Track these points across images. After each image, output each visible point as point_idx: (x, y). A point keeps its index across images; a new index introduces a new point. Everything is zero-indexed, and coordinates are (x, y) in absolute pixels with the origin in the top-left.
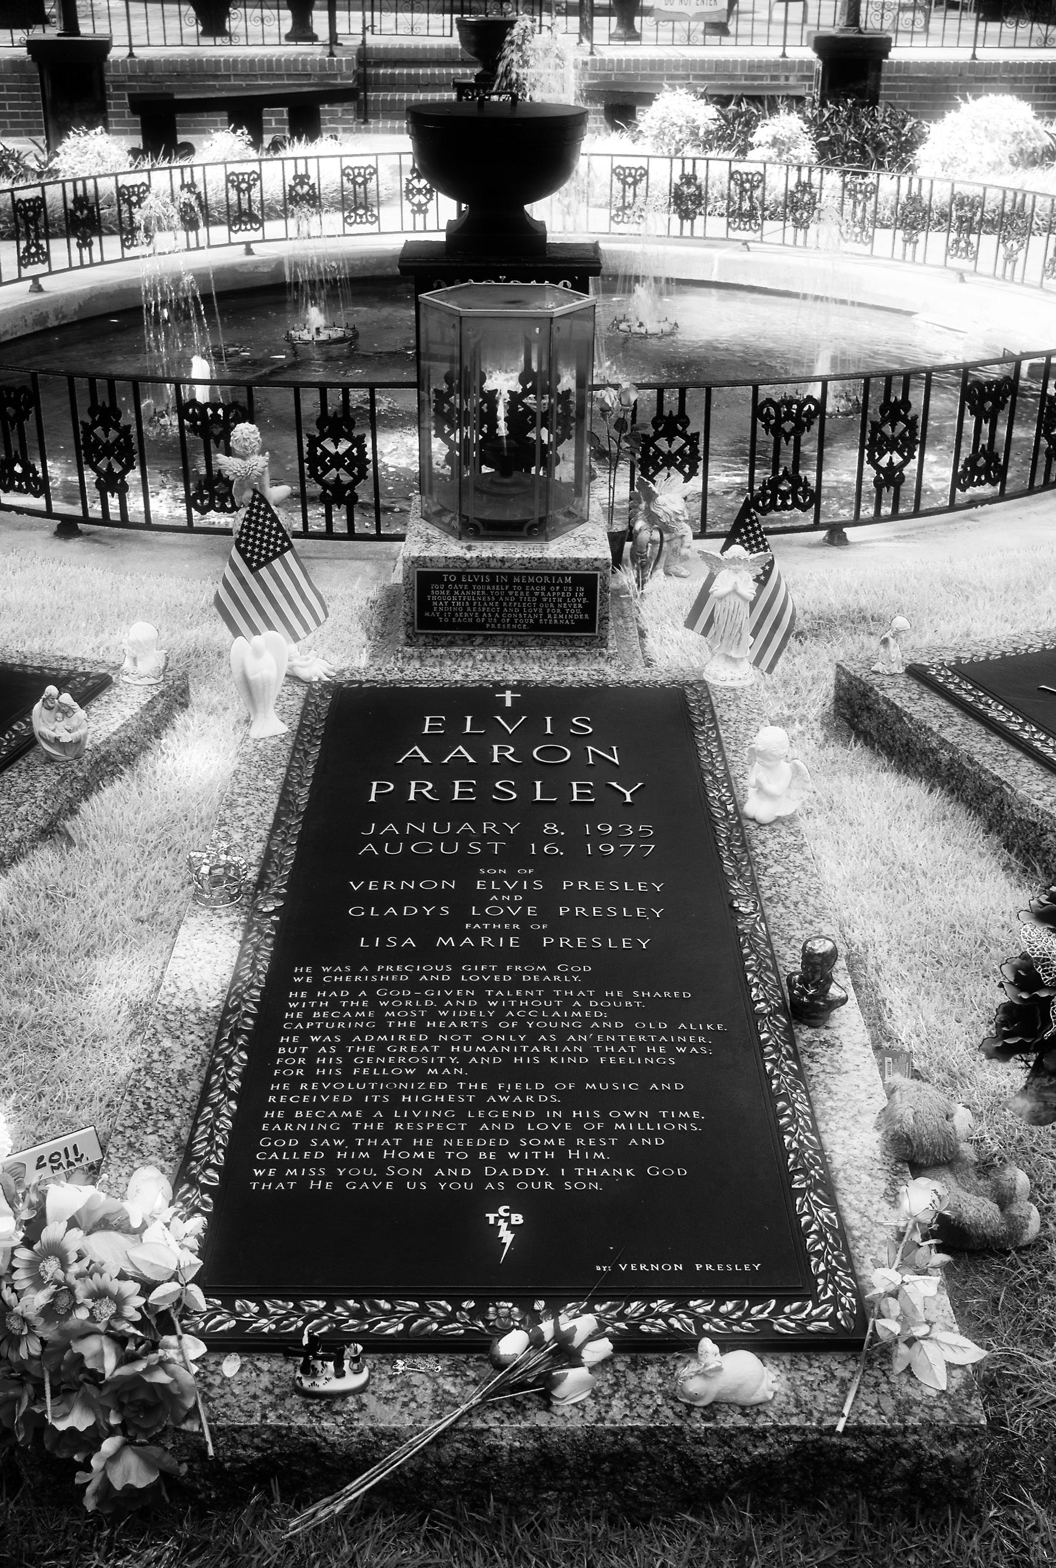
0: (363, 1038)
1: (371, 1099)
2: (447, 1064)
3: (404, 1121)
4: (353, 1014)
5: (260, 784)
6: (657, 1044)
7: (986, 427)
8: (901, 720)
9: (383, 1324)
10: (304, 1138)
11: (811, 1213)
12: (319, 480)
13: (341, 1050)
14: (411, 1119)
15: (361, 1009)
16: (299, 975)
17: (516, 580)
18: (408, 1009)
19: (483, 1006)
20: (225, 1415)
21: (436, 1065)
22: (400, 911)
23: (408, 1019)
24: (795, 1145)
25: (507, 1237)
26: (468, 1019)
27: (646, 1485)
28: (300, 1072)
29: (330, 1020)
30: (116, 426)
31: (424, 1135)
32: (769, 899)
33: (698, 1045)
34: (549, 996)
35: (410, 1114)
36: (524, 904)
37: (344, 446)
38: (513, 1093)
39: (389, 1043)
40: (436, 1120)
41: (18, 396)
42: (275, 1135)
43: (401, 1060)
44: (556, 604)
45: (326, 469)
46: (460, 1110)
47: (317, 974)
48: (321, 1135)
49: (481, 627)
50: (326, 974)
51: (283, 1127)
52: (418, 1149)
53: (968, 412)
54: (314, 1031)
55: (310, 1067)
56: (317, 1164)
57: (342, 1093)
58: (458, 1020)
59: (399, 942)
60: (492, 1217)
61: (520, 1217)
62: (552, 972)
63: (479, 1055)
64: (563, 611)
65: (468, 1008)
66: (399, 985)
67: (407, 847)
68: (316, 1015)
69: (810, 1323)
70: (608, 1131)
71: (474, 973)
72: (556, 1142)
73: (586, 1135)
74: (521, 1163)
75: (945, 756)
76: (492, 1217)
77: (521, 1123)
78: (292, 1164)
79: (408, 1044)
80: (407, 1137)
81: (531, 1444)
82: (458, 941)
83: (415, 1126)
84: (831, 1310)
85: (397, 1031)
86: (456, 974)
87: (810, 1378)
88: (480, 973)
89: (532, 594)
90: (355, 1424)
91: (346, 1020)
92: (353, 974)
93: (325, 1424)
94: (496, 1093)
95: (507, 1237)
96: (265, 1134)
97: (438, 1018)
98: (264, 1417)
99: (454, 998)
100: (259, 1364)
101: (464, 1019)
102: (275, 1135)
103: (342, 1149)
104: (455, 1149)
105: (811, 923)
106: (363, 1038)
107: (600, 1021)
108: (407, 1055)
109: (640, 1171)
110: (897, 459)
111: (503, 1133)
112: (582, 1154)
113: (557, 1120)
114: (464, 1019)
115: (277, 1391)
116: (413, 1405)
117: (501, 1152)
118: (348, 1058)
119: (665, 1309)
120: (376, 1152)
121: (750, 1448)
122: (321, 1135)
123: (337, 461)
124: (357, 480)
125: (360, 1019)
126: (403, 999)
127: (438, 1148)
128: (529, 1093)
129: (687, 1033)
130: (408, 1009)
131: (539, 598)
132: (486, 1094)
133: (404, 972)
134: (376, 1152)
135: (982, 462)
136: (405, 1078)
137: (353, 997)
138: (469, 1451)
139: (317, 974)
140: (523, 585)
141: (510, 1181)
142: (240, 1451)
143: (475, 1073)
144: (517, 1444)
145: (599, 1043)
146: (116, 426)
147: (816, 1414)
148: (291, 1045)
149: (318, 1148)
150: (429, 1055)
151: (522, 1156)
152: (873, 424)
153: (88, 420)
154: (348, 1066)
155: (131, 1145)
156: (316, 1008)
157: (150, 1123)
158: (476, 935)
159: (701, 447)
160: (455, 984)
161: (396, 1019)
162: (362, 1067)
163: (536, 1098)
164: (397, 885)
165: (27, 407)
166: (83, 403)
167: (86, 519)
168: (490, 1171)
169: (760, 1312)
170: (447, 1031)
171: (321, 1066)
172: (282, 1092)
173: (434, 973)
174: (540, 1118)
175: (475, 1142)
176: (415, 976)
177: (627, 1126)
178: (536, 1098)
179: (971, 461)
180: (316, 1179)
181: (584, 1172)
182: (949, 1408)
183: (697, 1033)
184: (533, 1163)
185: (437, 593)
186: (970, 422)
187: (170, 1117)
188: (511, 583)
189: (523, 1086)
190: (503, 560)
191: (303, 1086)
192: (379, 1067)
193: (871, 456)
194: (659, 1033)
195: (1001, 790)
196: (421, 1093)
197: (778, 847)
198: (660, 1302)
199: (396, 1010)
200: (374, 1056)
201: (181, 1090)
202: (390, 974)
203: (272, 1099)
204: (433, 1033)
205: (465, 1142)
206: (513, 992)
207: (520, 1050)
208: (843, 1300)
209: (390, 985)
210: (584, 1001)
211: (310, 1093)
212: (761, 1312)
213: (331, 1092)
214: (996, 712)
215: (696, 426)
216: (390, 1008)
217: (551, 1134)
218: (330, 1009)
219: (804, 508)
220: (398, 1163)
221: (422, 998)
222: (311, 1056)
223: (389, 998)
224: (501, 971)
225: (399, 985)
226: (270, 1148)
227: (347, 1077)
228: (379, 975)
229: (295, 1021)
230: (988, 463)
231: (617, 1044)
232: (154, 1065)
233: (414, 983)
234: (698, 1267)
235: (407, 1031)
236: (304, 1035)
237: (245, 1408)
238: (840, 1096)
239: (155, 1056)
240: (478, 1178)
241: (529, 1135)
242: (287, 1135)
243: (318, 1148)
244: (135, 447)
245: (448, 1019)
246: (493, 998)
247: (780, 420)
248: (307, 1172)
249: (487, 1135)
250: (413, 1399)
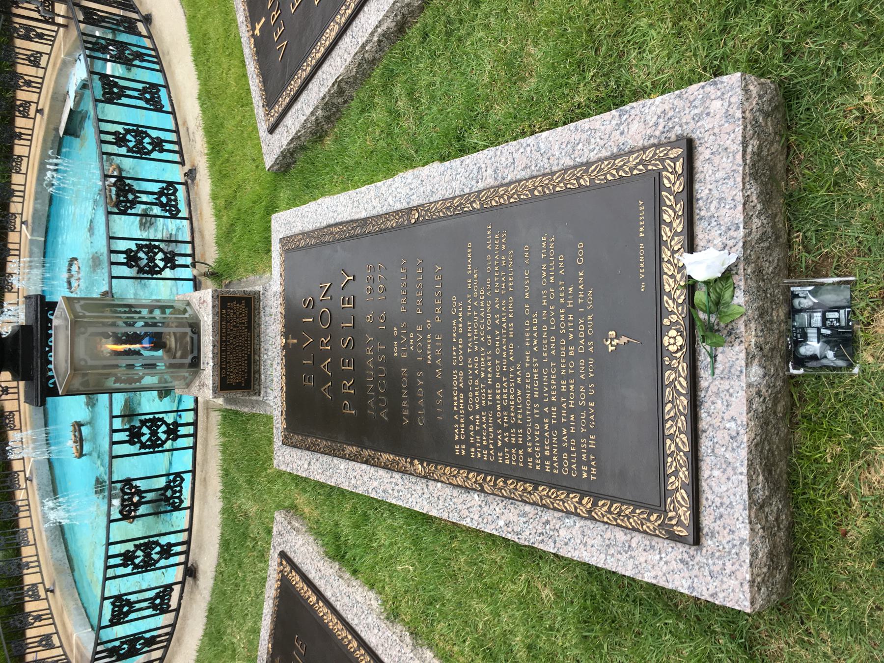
0: (499, 418)
1: (537, 414)
2: (514, 372)
3: (550, 396)
4: (484, 423)
5: (344, 472)
6: (500, 260)
7: (128, 92)
8: (299, 137)
9: (681, 408)
10: (561, 450)
11: (605, 175)
12: (164, 442)
13: (507, 429)
14: (548, 392)
15: (481, 419)
16: (460, 452)
17: (224, 338)
18: (480, 394)
19: (478, 354)
20: (742, 495)
21: (515, 378)
22: (421, 398)
23: (487, 394)
24: (562, 185)
25: (624, 340)
26: (486, 361)
27: (770, 262)
28: (520, 452)
29: (488, 435)
30: (134, 552)
31: (559, 385)
32: (408, 203)
33: (500, 238)
34: (471, 318)
35: (546, 392)
36: (415, 332)
37: (145, 430)
38: (532, 337)
39: (501, 404)
40: (549, 379)
41: (117, 606)
42: (561, 466)
43: (512, 397)
44: (237, 318)
45: (159, 439)
46: (541, 366)
47: (460, 442)
48: (560, 441)
49: (249, 356)
50: (459, 437)
51: (555, 462)
52: (568, 388)
53: (119, 101)
54: (495, 444)
55: (518, 446)
56: (578, 444)
57: (534, 430)
58: (487, 367)
59: (439, 398)
60: (611, 348)
61: (610, 333)
62: (456, 317)
63: (508, 356)
64: (240, 314)
65: (479, 362)
66: (466, 398)
67: (381, 394)
68: (485, 443)
69: (676, 172)
70: (555, 285)
71: (457, 358)
72: (562, 314)
73: (558, 297)
74: (576, 333)
75: (320, 113)
76: (611, 348)
77: (550, 333)
78: (579, 457)
79: (502, 394)
80: (560, 394)
81: (753, 325)
82: (439, 367)
83: (554, 390)
84: (668, 161)
85: (494, 400)
86: (458, 368)
87: (710, 172)
88: (458, 355)
89: (232, 330)
90: (745, 423)
91: (488, 427)
92: (459, 423)
93: (745, 440)
94: (532, 346)
95: (624, 340)
96: (560, 471)
97: (486, 378)
98: (741, 474)
99: (473, 369)
100: (706, 476)
101: (486, 364)
102: (561, 466)
103: (569, 430)
104: (567, 368)
105: (422, 181)
106: (499, 418)
107: (486, 291)
108: (509, 394)
109: (580, 268)
110: (147, 140)
111: (557, 344)
112: (570, 300)
113: (548, 313)
114: (486, 364)
115: (724, 466)
116: (731, 391)
117: (569, 343)
118: (511, 426)
119: (669, 253)
120: (570, 411)
121: (753, 204)
122: (560, 441)
123: (154, 433)
124: (164, 422)
125: (487, 420)
126: (474, 396)
127: (568, 377)
128: (531, 329)
129: (493, 245)
130: (480, 394)
131: (234, 326)
132: (532, 351)
133: (458, 396)
134: (570, 411)
135: (148, 96)
136: (523, 396)
137: (474, 423)
138: (756, 360)
139: (460, 442)
140: (227, 335)
141: (587, 339)
142: (760, 486)
143: (520, 358)
144: (753, 333)
145: (500, 292)
146: (134, 552)
147: (735, 167)
148: (503, 456)
149: (569, 442)
150: (508, 381)
151: (571, 332)
152: (128, 151)
153: (131, 567)
154: (517, 426)
155: (566, 544)
156: (481, 442)
157: (551, 533)
158: (434, 358)
159: (144, 243)
160: (465, 368)
161: (487, 400)
162: (517, 419)
163: (535, 325)
164: (405, 399)
165: (123, 600)
166: (121, 571)
167: (185, 563)
168: (581, 349)
169: (669, 199)
170: (494, 373)
171: (517, 440)
172: (534, 462)
173: (458, 380)
174: (547, 322)
175: (563, 358)
176: (460, 390)
177: (551, 276)
178: (535, 325)
179: (147, 101)
180: (589, 444)
181: (581, 298)
182: (730, 93)
183: (493, 239)
184: (576, 326)
185: (232, 380)
186: (124, 100)
187: (548, 522)
188: (225, 341)
189: (527, 332)
190: (214, 346)
191: (529, 450)
192: (517, 409)
193: (146, 154)
194: (493, 260)
195: (340, 82)
196: (533, 387)
197: (377, 200)
198: (664, 256)
199: (481, 400)
200: (510, 412)
201: (531, 516)
202: (459, 403)
203: (538, 467)
204: (495, 380)
205: (563, 363)
206: (469, 337)
207: (504, 334)
208: (661, 155)
209: (466, 403)
210: (476, 299)
211: (533, 446)
212: (670, 200)
213: (533, 435)
214: (295, 85)
215: (132, 245)
216: (480, 403)
217: (557, 316)
218: (481, 435)
219: (176, 190)
220: (577, 399)
221: (474, 386)
222: (510, 446)
223: (474, 404)
224: (457, 344)
225: (466, 398)
226: (568, 468)
227: (524, 427)
228: (459, 409)
229: (489, 454)
230: (148, 93)
231: (500, 282)
232: (515, 530)
233: (465, 391)
234: (641, 235)
235: (494, 394)
236: (497, 449)
237: (736, 484)
238: (528, 162)
239: (510, 529)
240: (586, 356)
241: (558, 328)
242: (561, 460)
243: (569, 442)
244: (146, 540)
245: (486, 372)
246: (473, 348)
248: (584, 448)
249: (558, 351)
250: (728, 391)
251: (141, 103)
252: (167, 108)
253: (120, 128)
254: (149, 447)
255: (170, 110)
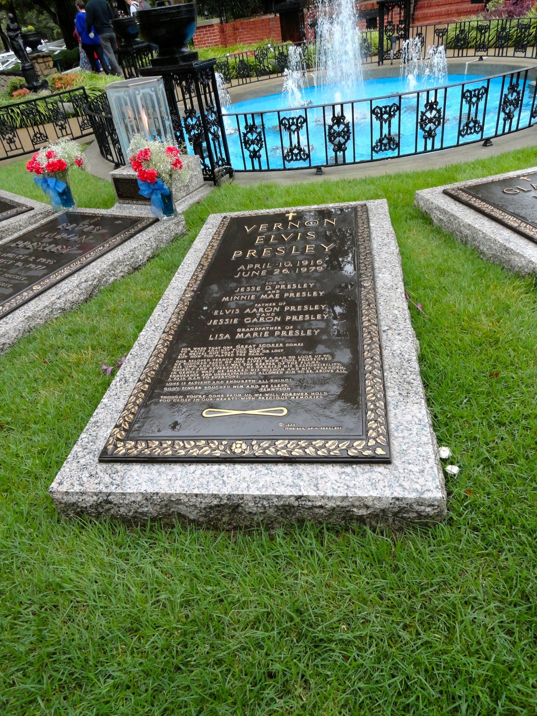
12: (248, 149)
247: (382, 114)
251: (464, 121)
252: (462, 140)
253: (441, 105)
254: (244, 139)
255: (460, 143)
